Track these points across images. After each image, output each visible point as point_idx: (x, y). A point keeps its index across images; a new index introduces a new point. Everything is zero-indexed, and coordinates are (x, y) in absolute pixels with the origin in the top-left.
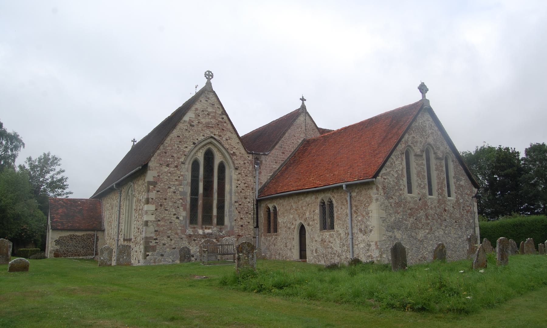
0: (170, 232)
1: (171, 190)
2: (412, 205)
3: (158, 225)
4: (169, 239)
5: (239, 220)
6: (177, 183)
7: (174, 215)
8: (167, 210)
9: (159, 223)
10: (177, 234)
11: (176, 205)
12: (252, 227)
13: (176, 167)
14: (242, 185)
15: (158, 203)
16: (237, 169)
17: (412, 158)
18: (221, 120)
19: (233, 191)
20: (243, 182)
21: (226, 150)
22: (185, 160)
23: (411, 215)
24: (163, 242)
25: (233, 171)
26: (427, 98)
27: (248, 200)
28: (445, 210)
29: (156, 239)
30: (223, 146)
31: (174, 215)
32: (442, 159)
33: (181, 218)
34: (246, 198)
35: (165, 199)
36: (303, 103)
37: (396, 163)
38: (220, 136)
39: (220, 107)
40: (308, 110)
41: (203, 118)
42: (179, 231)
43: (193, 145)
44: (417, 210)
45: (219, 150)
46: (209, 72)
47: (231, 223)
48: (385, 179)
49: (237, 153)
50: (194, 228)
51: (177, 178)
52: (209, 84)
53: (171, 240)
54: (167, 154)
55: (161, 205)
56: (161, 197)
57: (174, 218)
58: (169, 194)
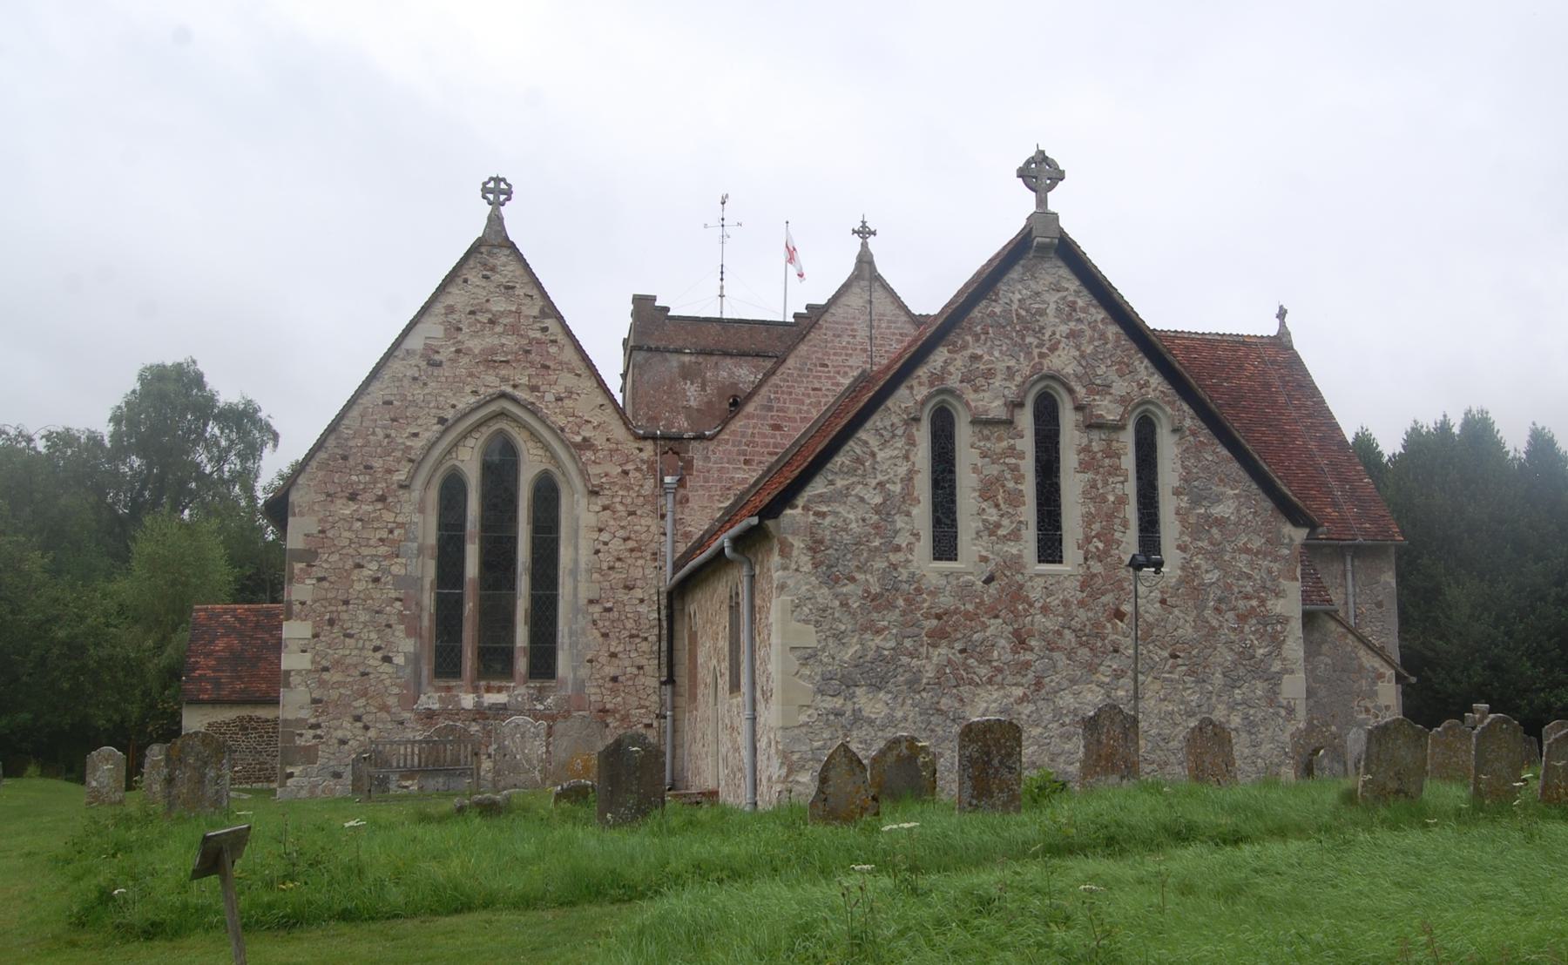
0: (362, 702)
1: (366, 572)
2: (946, 601)
3: (322, 684)
4: (359, 724)
5: (603, 659)
6: (383, 550)
7: (376, 649)
8: (350, 636)
9: (326, 676)
10: (384, 708)
11: (382, 619)
12: (654, 683)
13: (382, 499)
14: (616, 545)
15: (321, 615)
16: (596, 493)
17: (964, 434)
18: (538, 335)
19: (582, 565)
20: (621, 533)
21: (559, 432)
22: (412, 476)
23: (938, 636)
24: (340, 734)
25: (583, 502)
26: (1051, 207)
27: (638, 593)
29: (317, 726)
30: (543, 421)
31: (376, 649)
32: (1118, 427)
33: (399, 660)
34: (629, 588)
35: (346, 603)
37: (880, 456)
38: (534, 389)
39: (534, 292)
40: (882, 269)
41: (475, 334)
42: (392, 701)
43: (437, 427)
44: (968, 616)
45: (533, 435)
46: (498, 180)
47: (575, 669)
48: (823, 515)
49: (599, 441)
50: (448, 689)
51: (384, 534)
52: (495, 221)
53: (366, 728)
54: (351, 462)
55: (331, 622)
56: (330, 595)
57: (374, 660)
58: (358, 587)
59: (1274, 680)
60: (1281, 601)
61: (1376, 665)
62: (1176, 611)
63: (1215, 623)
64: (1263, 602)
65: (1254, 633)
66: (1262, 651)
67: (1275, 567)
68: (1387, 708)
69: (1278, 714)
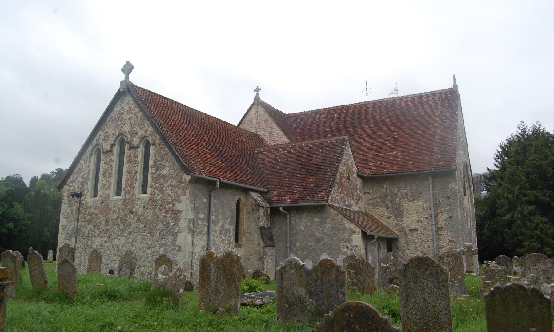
2: (92, 210)
23: (90, 221)
28: (132, 212)
32: (137, 147)
36: (257, 94)
37: (84, 167)
44: (97, 215)
48: (70, 186)
59: (175, 235)
60: (180, 204)
61: (352, 227)
62: (147, 210)
63: (158, 214)
64: (174, 205)
65: (170, 217)
66: (171, 224)
67: (179, 191)
68: (357, 246)
69: (175, 249)
